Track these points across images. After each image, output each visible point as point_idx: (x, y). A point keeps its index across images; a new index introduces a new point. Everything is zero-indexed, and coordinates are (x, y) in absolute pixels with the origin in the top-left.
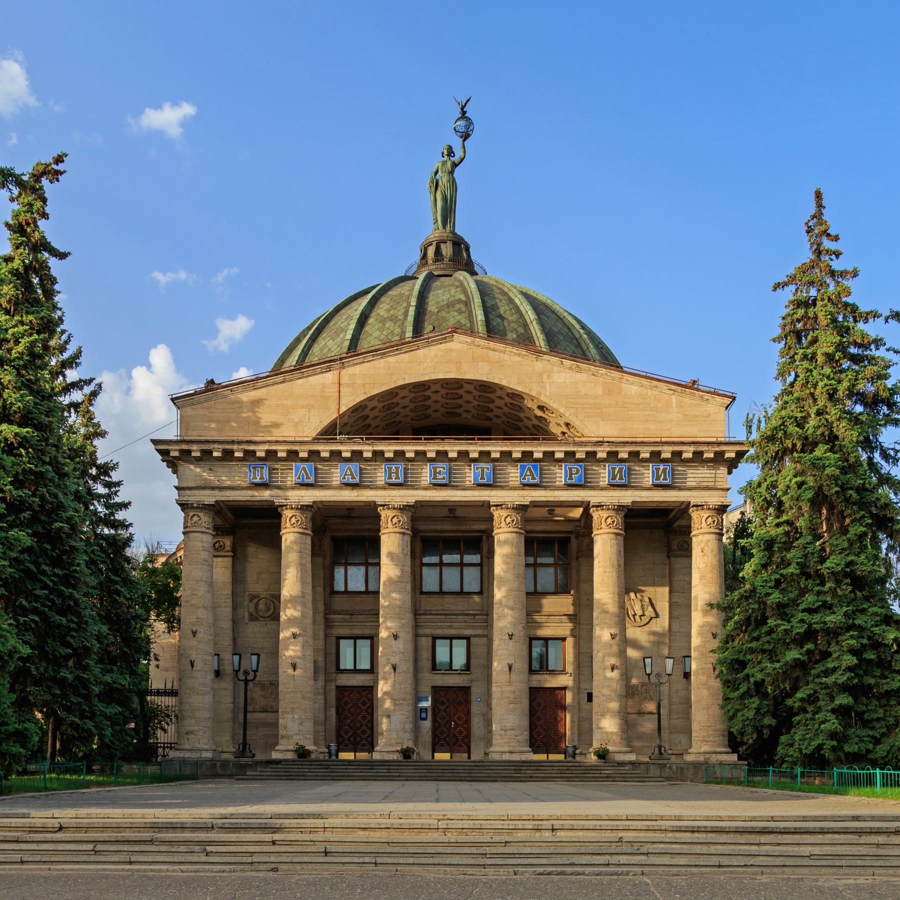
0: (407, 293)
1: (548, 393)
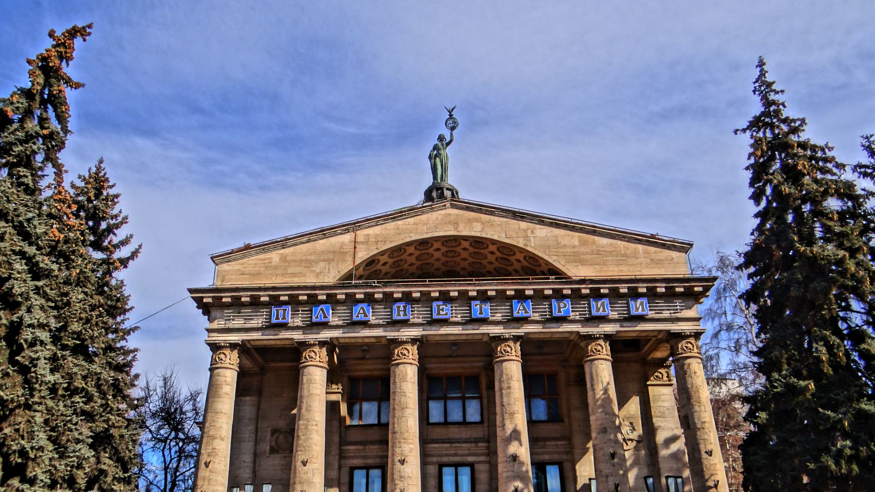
1: (533, 245)
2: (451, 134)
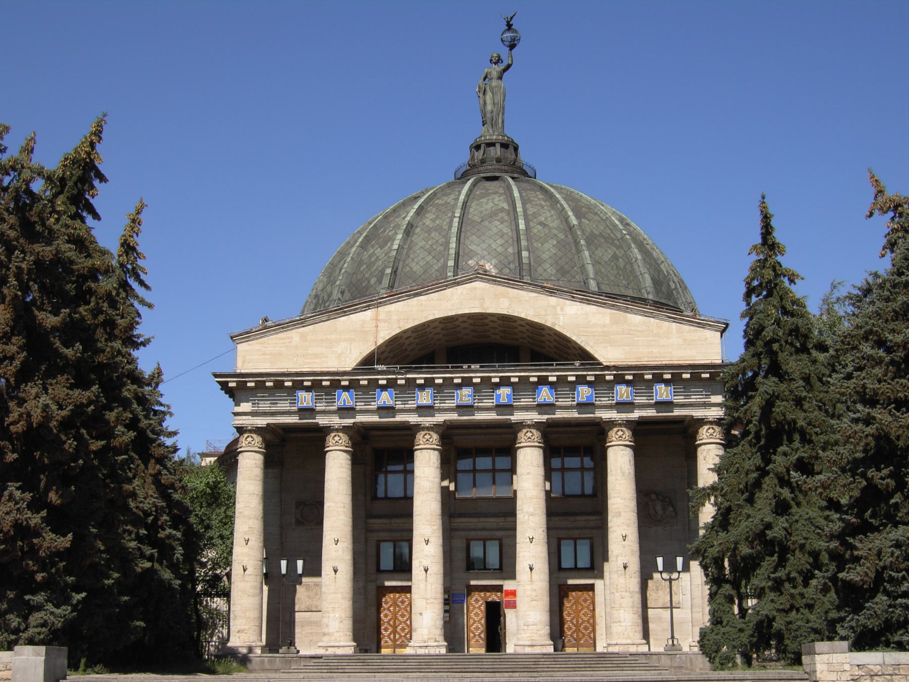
1: (561, 324)
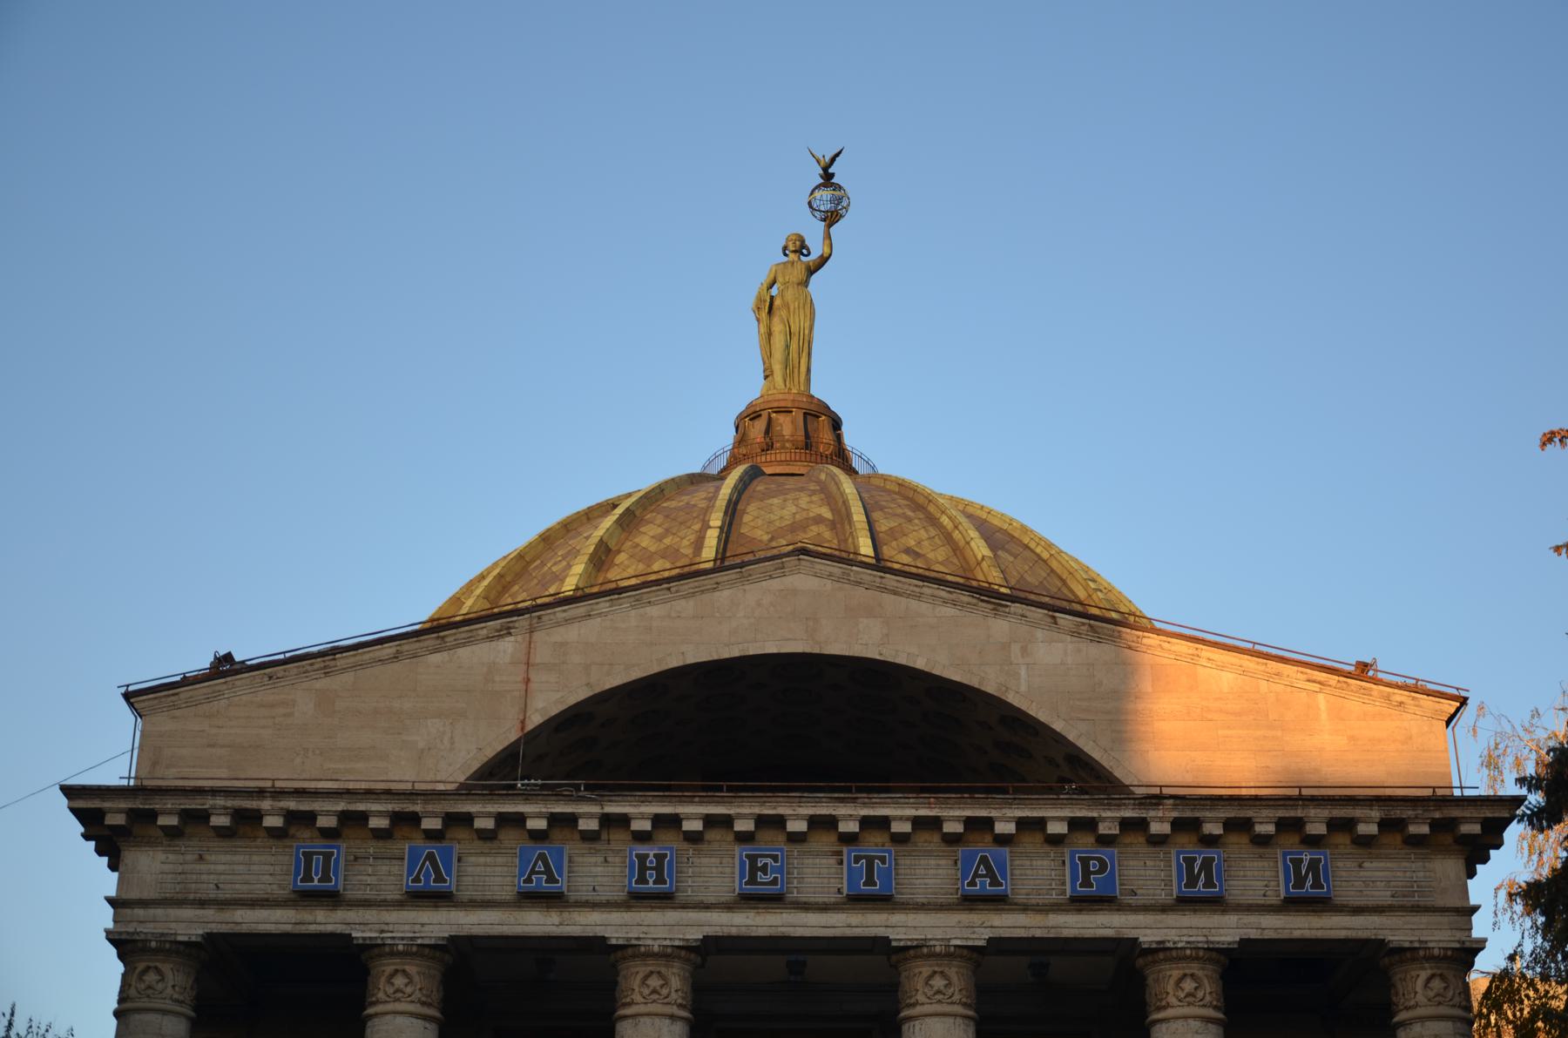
0: (703, 504)
1: (1023, 688)
2: (828, 236)
